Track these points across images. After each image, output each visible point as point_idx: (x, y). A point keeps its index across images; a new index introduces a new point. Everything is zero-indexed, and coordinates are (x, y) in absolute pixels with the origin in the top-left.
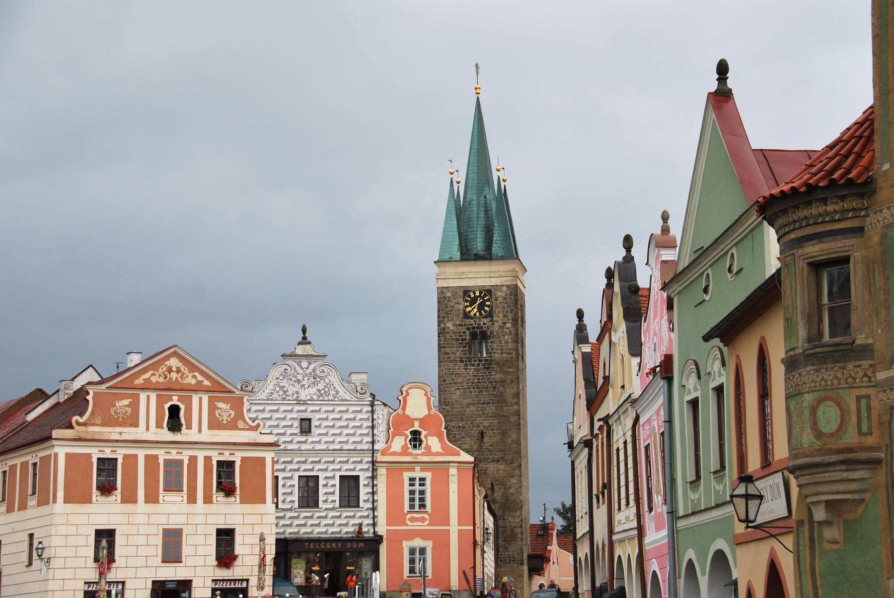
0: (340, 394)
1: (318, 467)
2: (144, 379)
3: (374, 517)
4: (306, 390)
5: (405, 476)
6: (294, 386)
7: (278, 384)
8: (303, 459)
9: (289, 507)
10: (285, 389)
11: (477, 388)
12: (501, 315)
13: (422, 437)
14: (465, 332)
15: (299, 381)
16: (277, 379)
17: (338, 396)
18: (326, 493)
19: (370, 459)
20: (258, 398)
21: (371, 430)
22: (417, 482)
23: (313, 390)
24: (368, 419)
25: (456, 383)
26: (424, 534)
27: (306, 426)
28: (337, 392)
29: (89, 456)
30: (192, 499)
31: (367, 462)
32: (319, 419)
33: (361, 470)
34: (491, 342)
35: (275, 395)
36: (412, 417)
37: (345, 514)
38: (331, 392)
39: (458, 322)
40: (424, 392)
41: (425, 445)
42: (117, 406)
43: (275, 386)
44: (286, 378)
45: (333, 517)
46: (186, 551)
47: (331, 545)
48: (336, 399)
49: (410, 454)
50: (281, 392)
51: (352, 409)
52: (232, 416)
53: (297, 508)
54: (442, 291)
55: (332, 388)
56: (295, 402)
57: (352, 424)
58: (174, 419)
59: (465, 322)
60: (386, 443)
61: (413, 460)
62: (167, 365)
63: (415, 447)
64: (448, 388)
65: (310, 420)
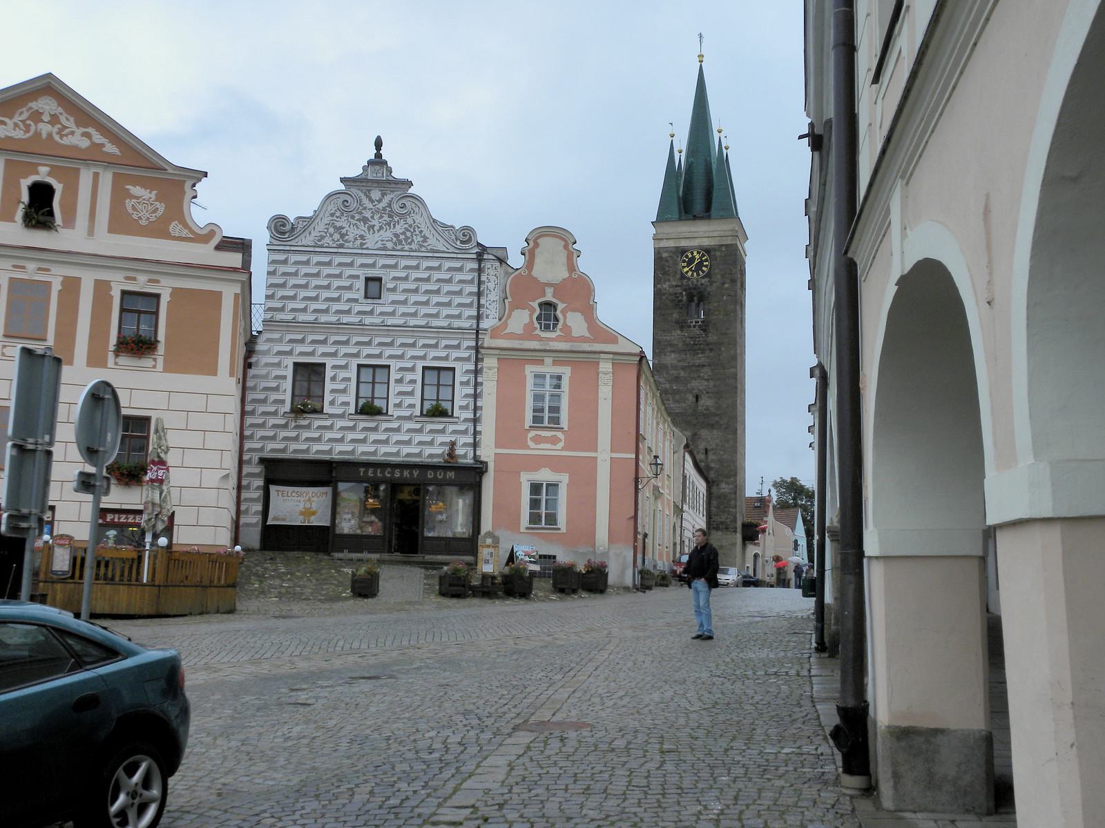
0: (429, 242)
1: (388, 351)
3: (476, 433)
4: (377, 235)
6: (358, 228)
7: (333, 224)
8: (366, 339)
9: (340, 411)
10: (344, 231)
13: (558, 313)
14: (681, 294)
15: (365, 220)
16: (332, 215)
17: (426, 244)
18: (400, 393)
19: (473, 343)
20: (299, 244)
21: (475, 298)
23: (387, 234)
24: (471, 282)
26: (555, 463)
27: (373, 286)
28: (425, 239)
31: (468, 348)
32: (395, 279)
33: (457, 359)
35: (327, 240)
36: (543, 280)
37: (429, 427)
39: (674, 283)
40: (564, 243)
45: (409, 431)
47: (402, 473)
48: (423, 249)
49: (539, 339)
50: (337, 236)
51: (448, 264)
52: (160, 213)
53: (351, 414)
55: (417, 233)
60: (500, 320)
61: (542, 348)
62: (31, 108)
65: (379, 280)
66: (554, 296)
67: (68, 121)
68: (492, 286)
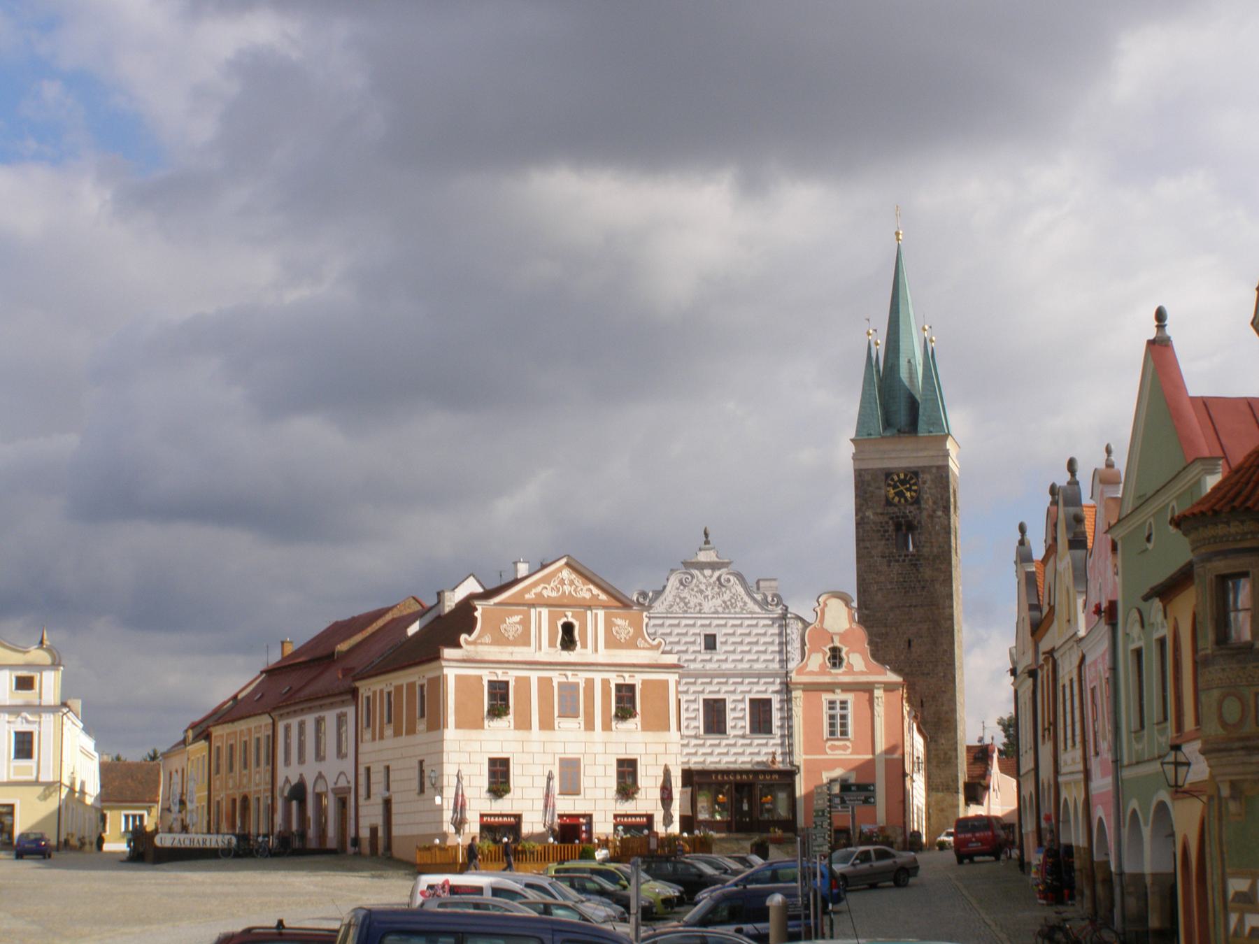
0: (748, 605)
1: (724, 688)
2: (535, 594)
4: (710, 602)
5: (823, 699)
6: (696, 597)
10: (687, 601)
12: (930, 501)
13: (843, 654)
14: (887, 523)
15: (701, 592)
16: (678, 589)
17: (746, 608)
18: (735, 718)
22: (838, 705)
23: (718, 601)
25: (877, 583)
27: (710, 643)
28: (745, 604)
29: (480, 678)
30: (590, 726)
32: (726, 634)
34: (919, 534)
35: (675, 608)
36: (831, 630)
38: (738, 603)
39: (879, 511)
42: (507, 622)
46: (585, 782)
48: (744, 612)
49: (830, 674)
50: (682, 604)
56: (699, 615)
58: (568, 638)
60: (802, 660)
62: (559, 577)
63: (834, 665)
67: (578, 581)
68: (794, 636)
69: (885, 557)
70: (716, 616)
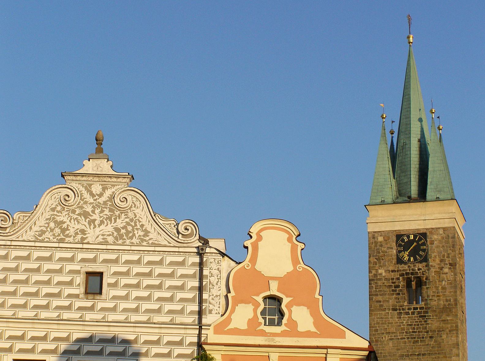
0: (151, 236)
4: (97, 229)
6: (78, 222)
7: (54, 218)
10: (65, 226)
11: (412, 338)
13: (283, 306)
14: (398, 279)
15: (86, 215)
16: (53, 210)
17: (147, 238)
19: (195, 340)
20: (20, 239)
23: (109, 228)
24: (193, 276)
28: (147, 233)
32: (115, 273)
34: (427, 288)
35: (48, 235)
36: (267, 272)
38: (136, 232)
39: (391, 268)
40: (288, 236)
41: (288, 320)
43: (47, 221)
44: (66, 210)
48: (145, 243)
49: (263, 333)
50: (57, 231)
54: (374, 235)
55: (139, 227)
56: (80, 246)
57: (169, 283)
59: (398, 267)
64: (380, 338)
65: (101, 274)
66: (278, 291)
69: (396, 310)
70: (104, 247)
